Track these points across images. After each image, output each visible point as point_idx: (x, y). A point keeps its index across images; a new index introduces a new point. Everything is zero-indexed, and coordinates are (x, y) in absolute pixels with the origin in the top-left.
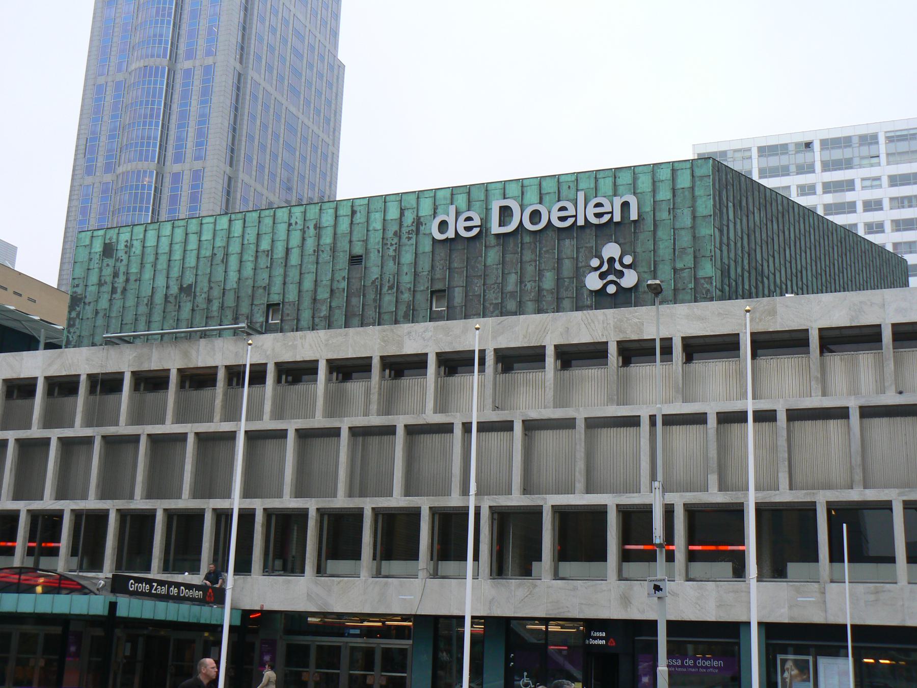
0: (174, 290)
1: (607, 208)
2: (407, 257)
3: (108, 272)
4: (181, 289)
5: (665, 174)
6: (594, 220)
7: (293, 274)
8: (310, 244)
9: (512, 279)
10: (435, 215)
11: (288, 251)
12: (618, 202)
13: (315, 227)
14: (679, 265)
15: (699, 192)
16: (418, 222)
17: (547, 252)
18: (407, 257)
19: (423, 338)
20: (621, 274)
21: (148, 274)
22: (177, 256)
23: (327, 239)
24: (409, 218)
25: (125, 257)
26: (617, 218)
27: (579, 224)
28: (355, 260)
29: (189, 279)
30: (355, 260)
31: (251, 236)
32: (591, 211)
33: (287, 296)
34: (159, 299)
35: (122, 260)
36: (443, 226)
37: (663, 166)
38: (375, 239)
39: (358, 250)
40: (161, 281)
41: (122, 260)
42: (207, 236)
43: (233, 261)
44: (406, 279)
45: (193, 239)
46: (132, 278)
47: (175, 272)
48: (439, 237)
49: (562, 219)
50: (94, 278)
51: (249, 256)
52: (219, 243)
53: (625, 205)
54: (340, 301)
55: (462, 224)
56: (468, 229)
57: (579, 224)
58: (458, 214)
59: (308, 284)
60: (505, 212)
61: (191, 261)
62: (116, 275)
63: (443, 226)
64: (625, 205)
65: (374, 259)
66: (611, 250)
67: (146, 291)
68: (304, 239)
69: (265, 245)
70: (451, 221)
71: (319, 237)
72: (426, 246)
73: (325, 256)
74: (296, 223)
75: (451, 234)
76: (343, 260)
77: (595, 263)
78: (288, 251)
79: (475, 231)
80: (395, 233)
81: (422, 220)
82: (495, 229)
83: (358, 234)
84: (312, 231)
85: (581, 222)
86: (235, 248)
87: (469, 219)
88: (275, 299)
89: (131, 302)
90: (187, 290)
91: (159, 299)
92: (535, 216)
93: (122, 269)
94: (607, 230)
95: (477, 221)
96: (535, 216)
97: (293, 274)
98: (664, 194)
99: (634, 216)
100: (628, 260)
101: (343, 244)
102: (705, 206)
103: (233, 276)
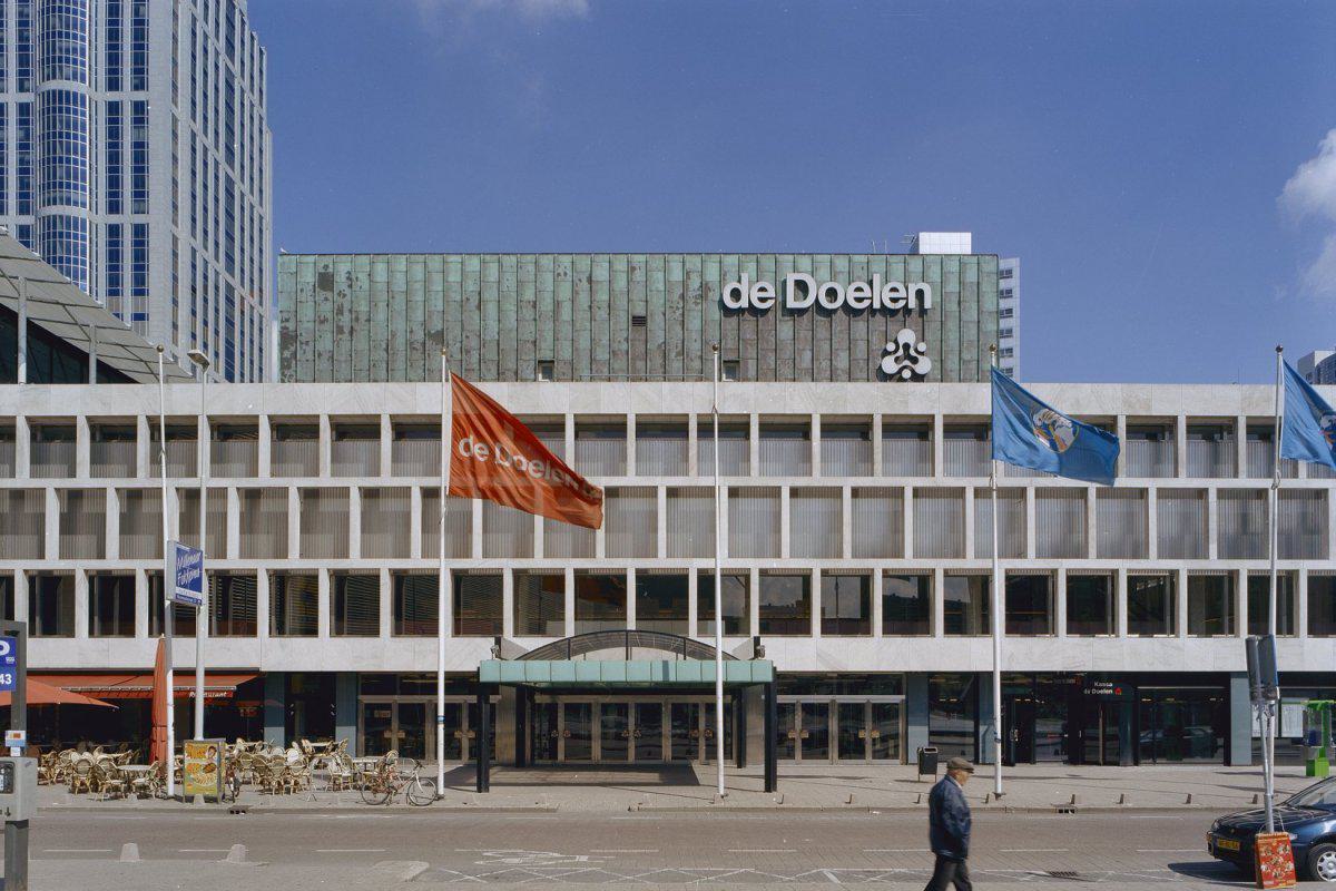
0: (419, 335)
1: (902, 293)
2: (694, 324)
3: (326, 309)
4: (427, 334)
5: (954, 267)
7: (566, 330)
8: (583, 299)
10: (722, 281)
11: (557, 304)
12: (913, 289)
13: (590, 280)
15: (984, 288)
16: (705, 287)
17: (841, 331)
21: (381, 315)
22: (419, 297)
23: (602, 296)
24: (695, 282)
25: (348, 291)
26: (913, 304)
27: (875, 307)
29: (436, 325)
30: (639, 321)
31: (510, 282)
32: (887, 296)
33: (561, 353)
34: (400, 342)
35: (345, 296)
37: (953, 258)
38: (657, 302)
39: (640, 311)
40: (400, 325)
41: (345, 296)
42: (454, 277)
43: (491, 309)
45: (437, 278)
46: (363, 318)
47: (419, 315)
49: (859, 300)
50: (307, 313)
51: (510, 307)
52: (471, 287)
53: (920, 294)
55: (755, 295)
56: (762, 300)
57: (875, 307)
58: (751, 284)
59: (584, 343)
61: (437, 304)
62: (340, 311)
63: (736, 294)
64: (920, 294)
65: (656, 324)
66: (907, 336)
67: (381, 334)
68: (575, 293)
69: (529, 295)
70: (744, 289)
72: (716, 314)
73: (602, 314)
74: (565, 274)
75: (744, 303)
76: (623, 320)
78: (557, 304)
79: (769, 304)
80: (683, 297)
81: (710, 285)
82: (791, 304)
83: (638, 293)
84: (585, 284)
85: (877, 305)
86: (491, 295)
87: (762, 289)
89: (361, 343)
90: (439, 337)
91: (400, 342)
92: (832, 293)
93: (347, 306)
95: (771, 293)
96: (832, 293)
97: (566, 330)
99: (928, 304)
101: (622, 302)
103: (493, 325)
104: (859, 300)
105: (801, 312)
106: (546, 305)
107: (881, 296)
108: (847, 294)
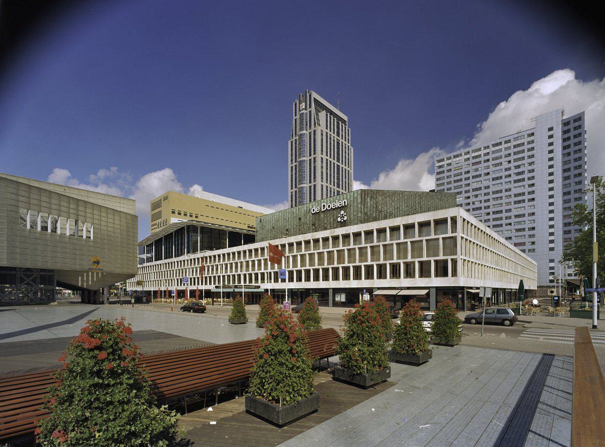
2: (308, 217)
3: (261, 225)
6: (339, 206)
9: (326, 220)
12: (343, 201)
14: (355, 214)
18: (308, 217)
19: (310, 236)
20: (344, 217)
23: (295, 215)
24: (308, 209)
28: (300, 219)
29: (274, 226)
36: (314, 210)
38: (303, 214)
44: (308, 222)
48: (313, 212)
54: (298, 227)
60: (324, 206)
63: (314, 210)
66: (342, 212)
71: (293, 215)
73: (295, 219)
75: (315, 212)
77: (339, 215)
82: (322, 210)
88: (287, 228)
94: (341, 208)
96: (329, 206)
98: (352, 199)
100: (345, 214)
102: (359, 201)
104: (334, 206)
105: (325, 211)
106: (287, 219)
107: (338, 205)
108: (332, 206)
